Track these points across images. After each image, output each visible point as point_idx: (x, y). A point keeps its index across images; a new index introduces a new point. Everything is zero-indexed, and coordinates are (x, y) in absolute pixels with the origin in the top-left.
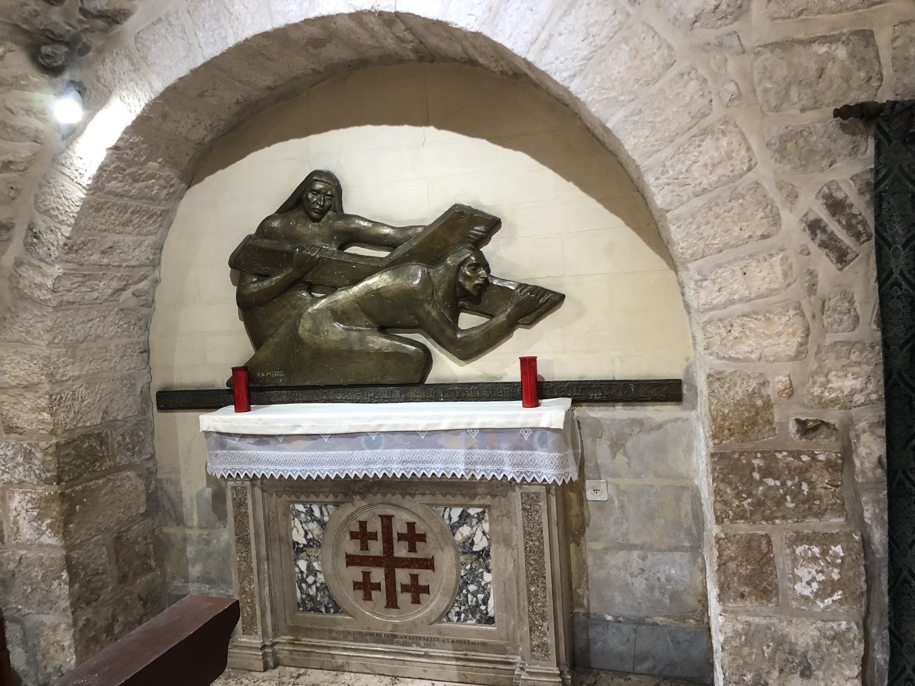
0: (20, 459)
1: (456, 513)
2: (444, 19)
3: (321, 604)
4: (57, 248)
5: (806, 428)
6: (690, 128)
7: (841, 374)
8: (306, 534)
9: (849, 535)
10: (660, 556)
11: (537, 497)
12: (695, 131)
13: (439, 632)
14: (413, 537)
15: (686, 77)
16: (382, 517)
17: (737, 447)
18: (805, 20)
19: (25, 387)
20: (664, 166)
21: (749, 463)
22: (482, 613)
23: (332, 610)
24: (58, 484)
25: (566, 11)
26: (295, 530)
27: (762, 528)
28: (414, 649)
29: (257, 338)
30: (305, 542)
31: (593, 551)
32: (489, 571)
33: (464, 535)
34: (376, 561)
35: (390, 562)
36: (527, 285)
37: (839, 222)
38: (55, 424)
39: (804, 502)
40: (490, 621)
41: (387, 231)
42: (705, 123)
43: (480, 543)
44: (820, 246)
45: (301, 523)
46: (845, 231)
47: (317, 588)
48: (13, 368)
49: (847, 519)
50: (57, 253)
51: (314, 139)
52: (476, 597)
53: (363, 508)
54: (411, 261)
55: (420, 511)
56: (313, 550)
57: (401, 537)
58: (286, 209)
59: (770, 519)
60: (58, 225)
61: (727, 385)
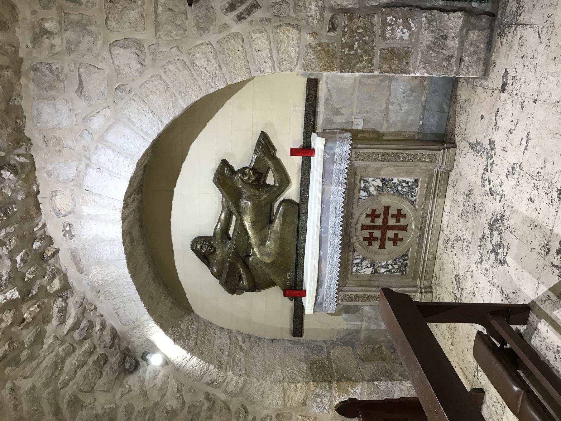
0: (319, 400)
1: (363, 193)
2: (129, 179)
3: (403, 263)
4: (219, 373)
5: (333, 28)
6: (190, 70)
7: (308, 10)
8: (367, 267)
9: (382, 13)
10: (392, 95)
11: (357, 153)
12: (191, 68)
13: (420, 206)
14: (373, 215)
15: (167, 70)
16: (362, 229)
17: (338, 60)
18: (146, 14)
19: (284, 394)
20: (206, 83)
21: (346, 55)
22: (413, 185)
23: (406, 258)
24: (332, 382)
25: (131, 123)
26: (366, 273)
27: (377, 52)
28: (428, 219)
29: (271, 284)
31: (387, 128)
32: (392, 180)
34: (384, 234)
35: (385, 228)
36: (255, 150)
37: (239, 6)
38: (303, 381)
39: (366, 32)
40: (417, 181)
41: (223, 215)
42: (188, 63)
43: (379, 183)
44: (249, 16)
46: (243, 4)
47: (395, 264)
48: (275, 399)
49: (376, 14)
50: (221, 373)
51: (175, 248)
52: (404, 187)
53: (357, 238)
54: (239, 205)
55: (361, 211)
56: (376, 264)
57: (372, 221)
58: (209, 264)
60: (209, 371)
61: (310, 63)
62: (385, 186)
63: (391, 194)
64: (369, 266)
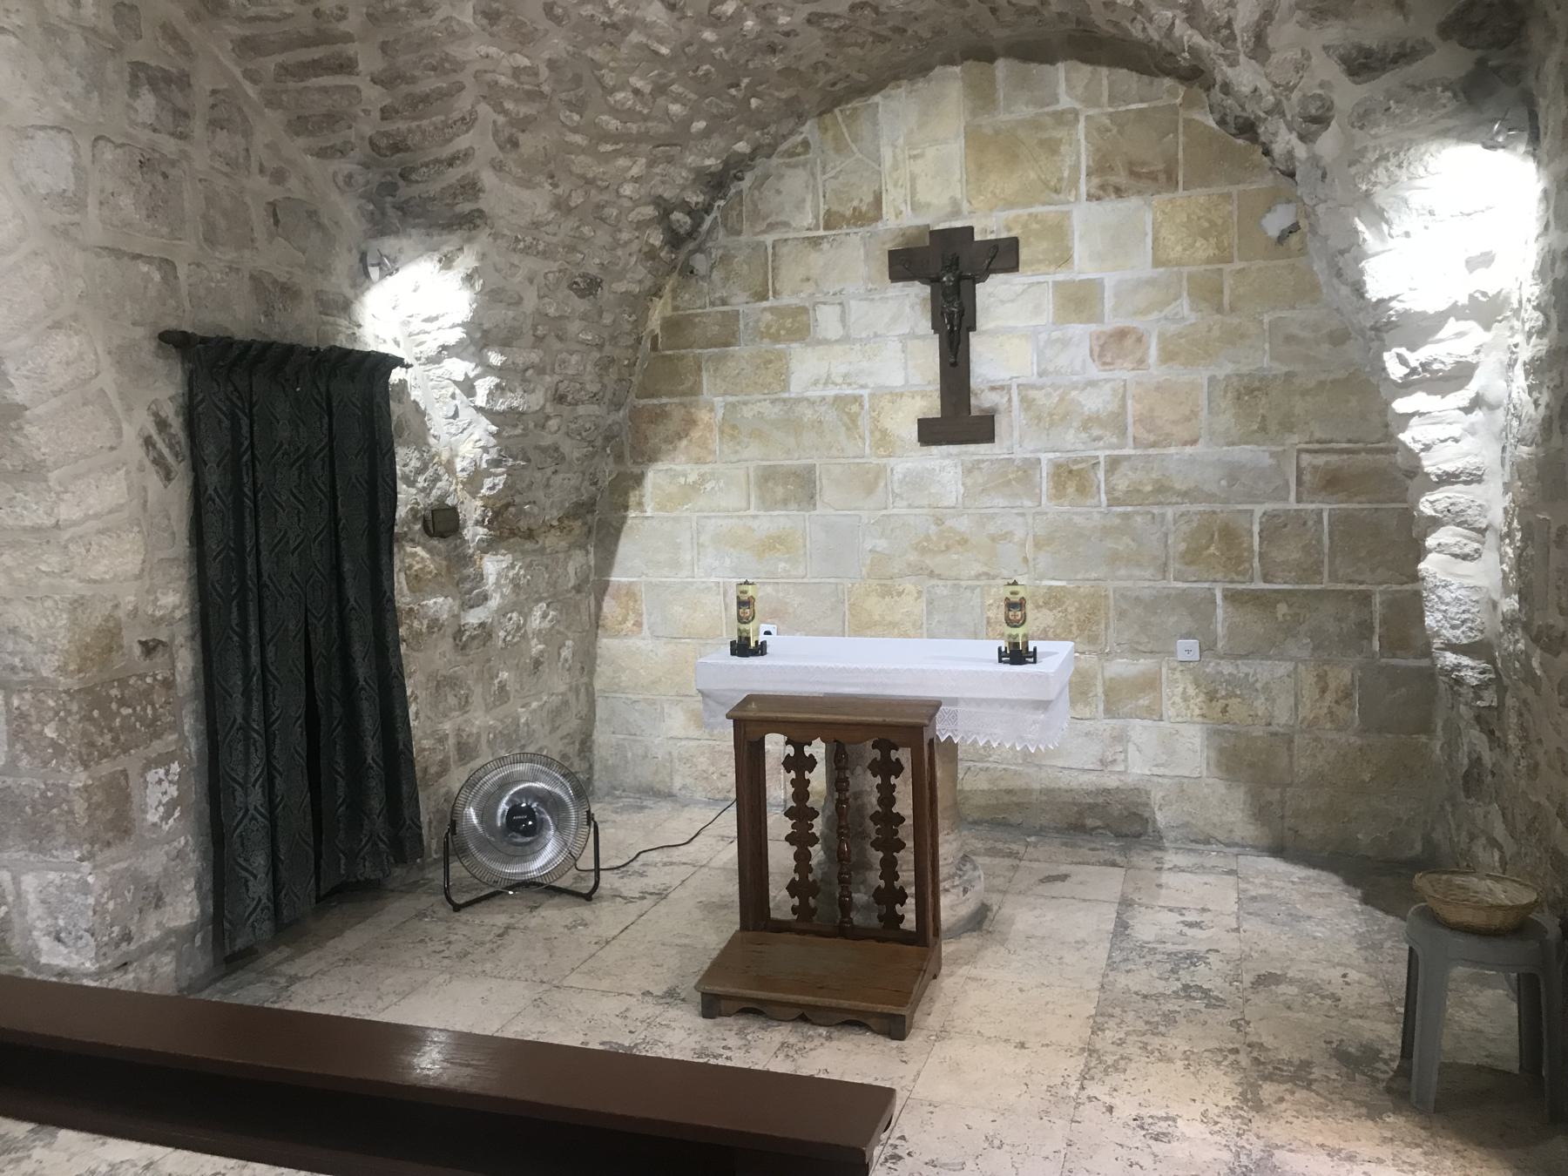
5: (149, 648)
12: (49, 322)
27: (123, 762)
59: (125, 751)
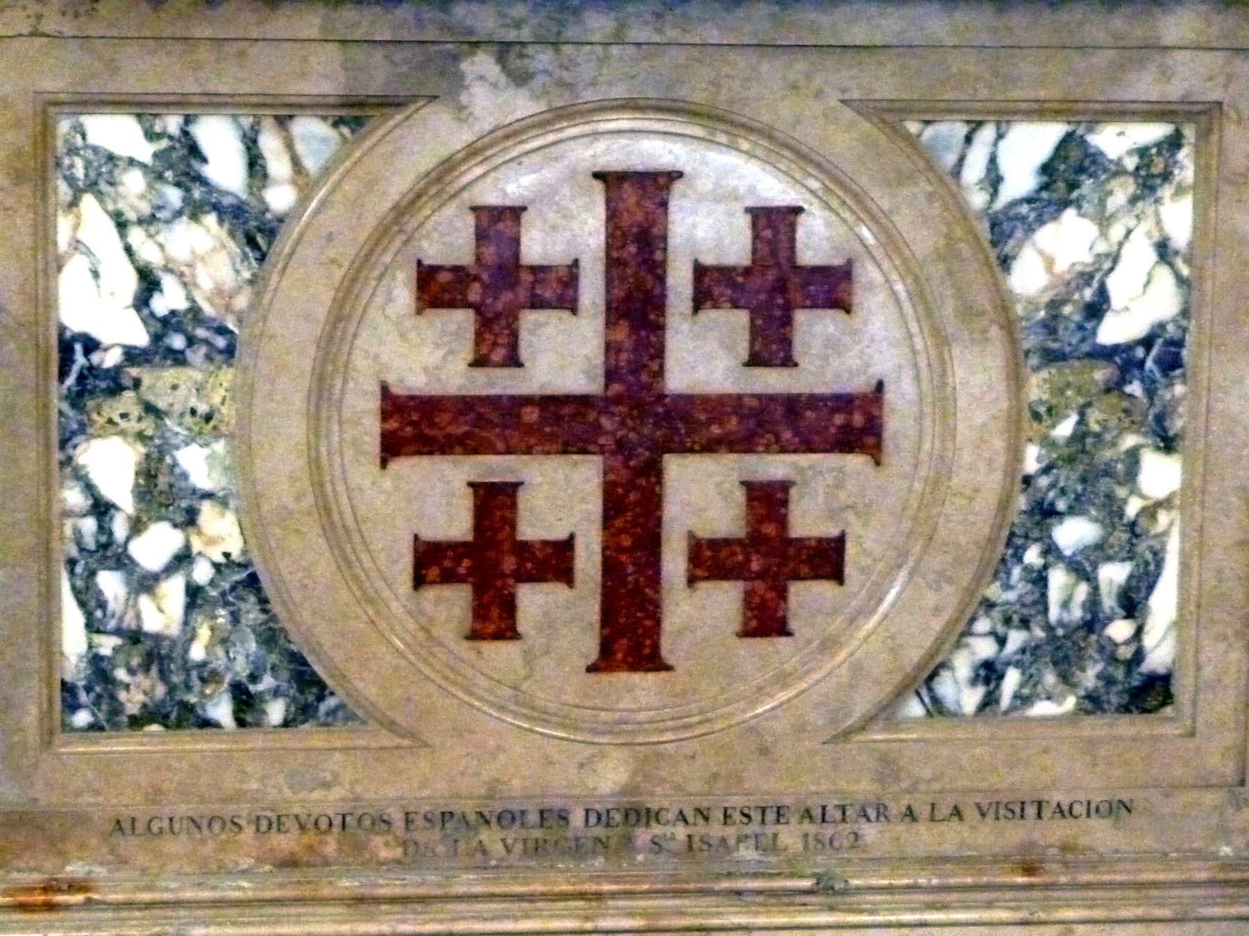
8: (149, 282)
16: (610, 180)
22: (1113, 659)
23: (276, 711)
30: (141, 338)
32: (1168, 444)
33: (1061, 266)
45: (122, 225)
47: (194, 593)
53: (513, 132)
62: (1101, 374)
63: (1016, 455)
64: (161, 305)
